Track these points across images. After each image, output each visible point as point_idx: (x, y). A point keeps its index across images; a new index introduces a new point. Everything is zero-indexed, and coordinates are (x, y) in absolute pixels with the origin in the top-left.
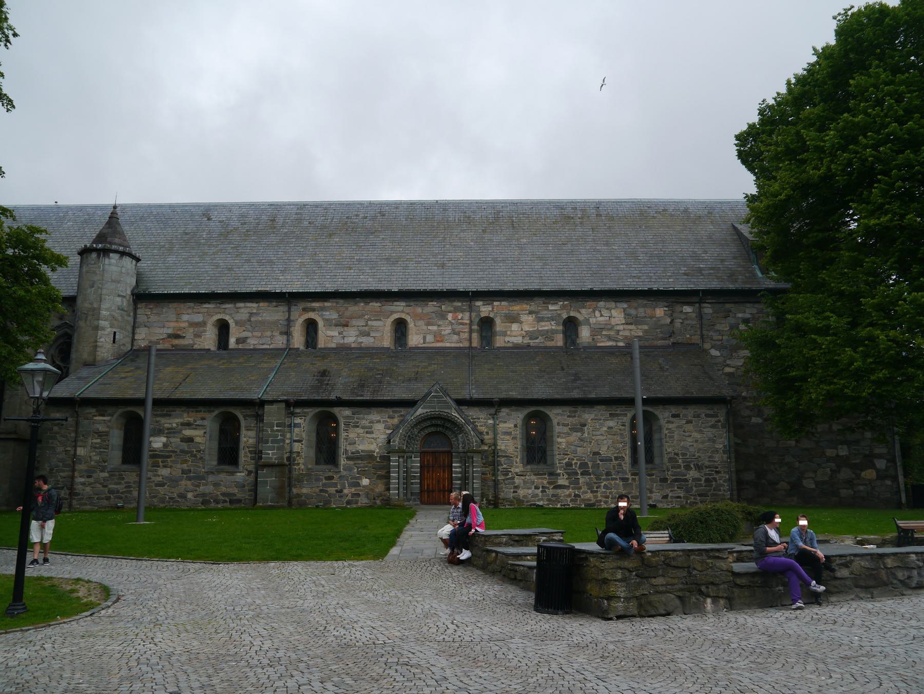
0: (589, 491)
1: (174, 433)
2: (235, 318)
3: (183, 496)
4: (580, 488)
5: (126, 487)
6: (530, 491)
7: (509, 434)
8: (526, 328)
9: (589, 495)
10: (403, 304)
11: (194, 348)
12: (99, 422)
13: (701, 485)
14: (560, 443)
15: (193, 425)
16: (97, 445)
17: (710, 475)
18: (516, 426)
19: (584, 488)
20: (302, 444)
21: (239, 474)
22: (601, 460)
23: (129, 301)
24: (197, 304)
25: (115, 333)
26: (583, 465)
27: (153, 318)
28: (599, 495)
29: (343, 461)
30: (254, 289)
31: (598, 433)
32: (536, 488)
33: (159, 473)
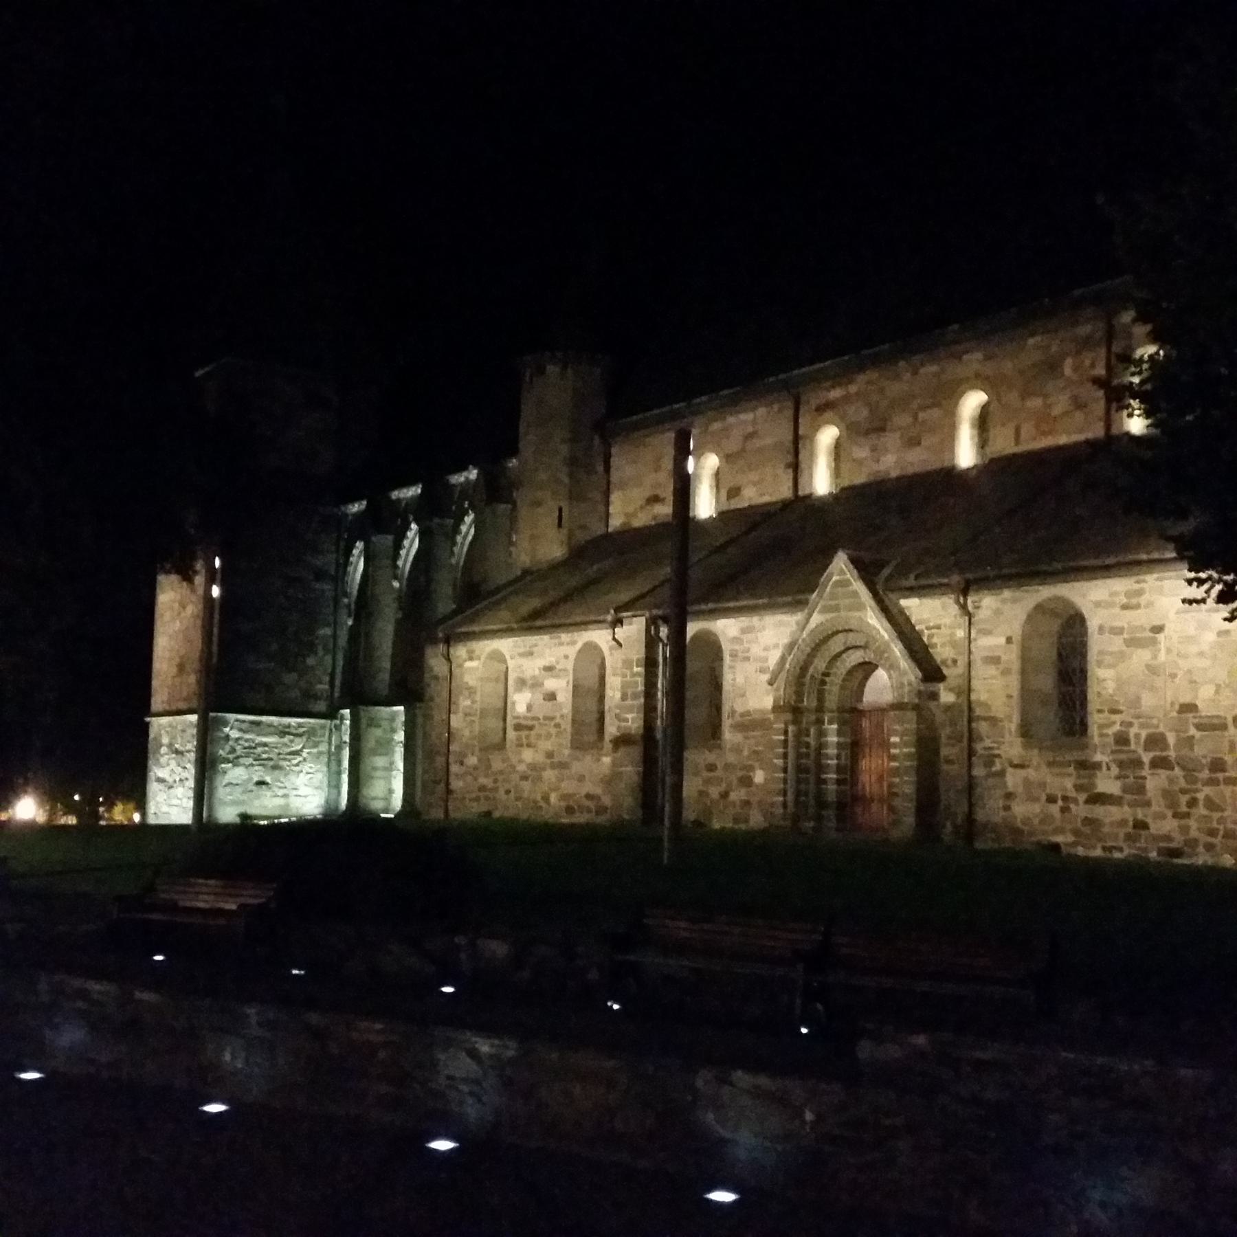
0: (1169, 813)
3: (546, 798)
6: (1036, 808)
9: (1169, 825)
10: (979, 355)
18: (1009, 640)
19: (1158, 805)
22: (1199, 727)
25: (560, 510)
26: (1155, 741)
28: (1193, 824)
29: (729, 736)
32: (1051, 799)
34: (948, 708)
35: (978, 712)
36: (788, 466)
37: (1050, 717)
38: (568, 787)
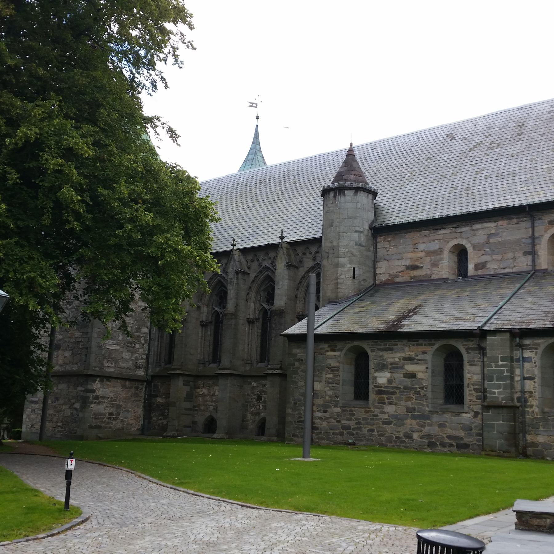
1: (397, 368)
2: (472, 243)
3: (409, 436)
5: (357, 424)
11: (432, 278)
12: (331, 357)
15: (414, 359)
16: (330, 380)
20: (535, 382)
21: (464, 415)
23: (367, 236)
24: (432, 231)
25: (354, 269)
27: (392, 251)
30: (491, 206)
33: (385, 410)
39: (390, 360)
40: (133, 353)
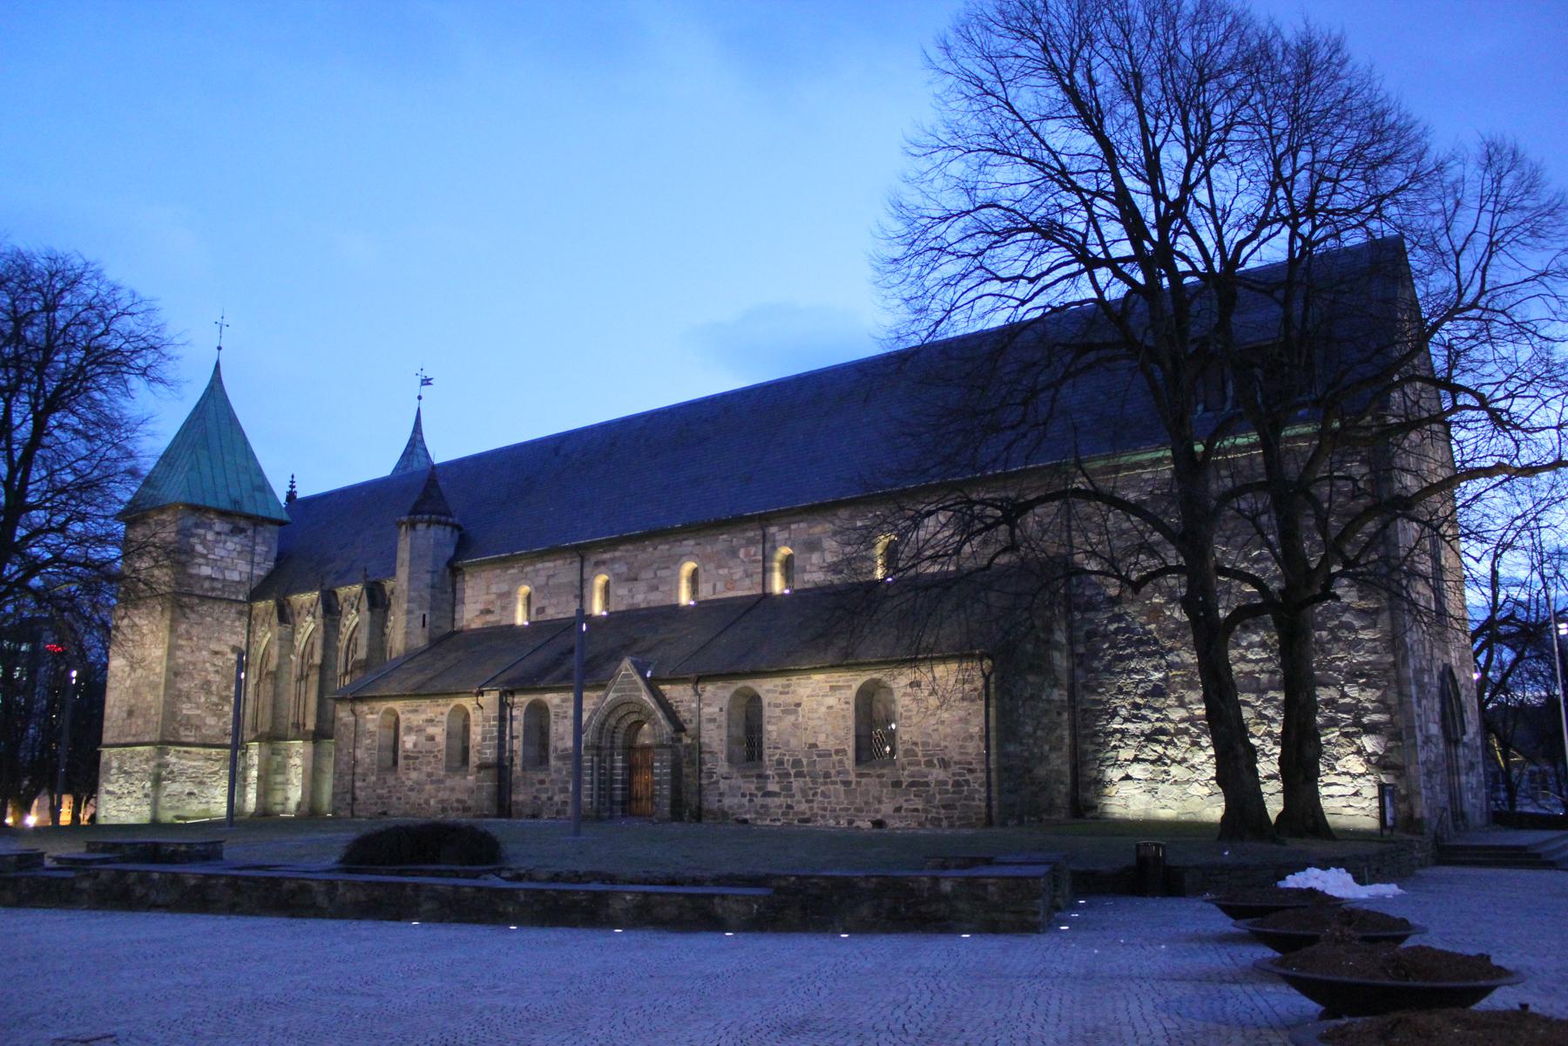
3: (427, 802)
4: (792, 796)
6: (736, 801)
7: (714, 720)
8: (830, 558)
9: (804, 806)
10: (691, 542)
13: (947, 792)
14: (769, 732)
17: (960, 775)
18: (721, 710)
19: (798, 796)
22: (819, 756)
28: (815, 805)
29: (553, 762)
31: (815, 715)
32: (744, 795)
34: (687, 746)
35: (705, 749)
36: (576, 597)
37: (741, 751)
38: (443, 795)
39: (415, 723)
40: (219, 718)
